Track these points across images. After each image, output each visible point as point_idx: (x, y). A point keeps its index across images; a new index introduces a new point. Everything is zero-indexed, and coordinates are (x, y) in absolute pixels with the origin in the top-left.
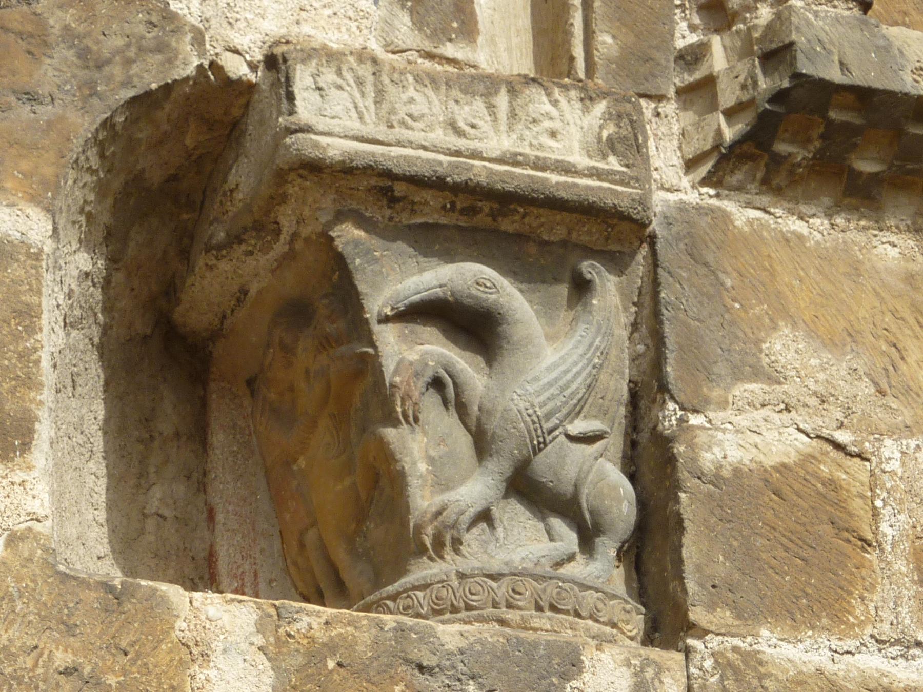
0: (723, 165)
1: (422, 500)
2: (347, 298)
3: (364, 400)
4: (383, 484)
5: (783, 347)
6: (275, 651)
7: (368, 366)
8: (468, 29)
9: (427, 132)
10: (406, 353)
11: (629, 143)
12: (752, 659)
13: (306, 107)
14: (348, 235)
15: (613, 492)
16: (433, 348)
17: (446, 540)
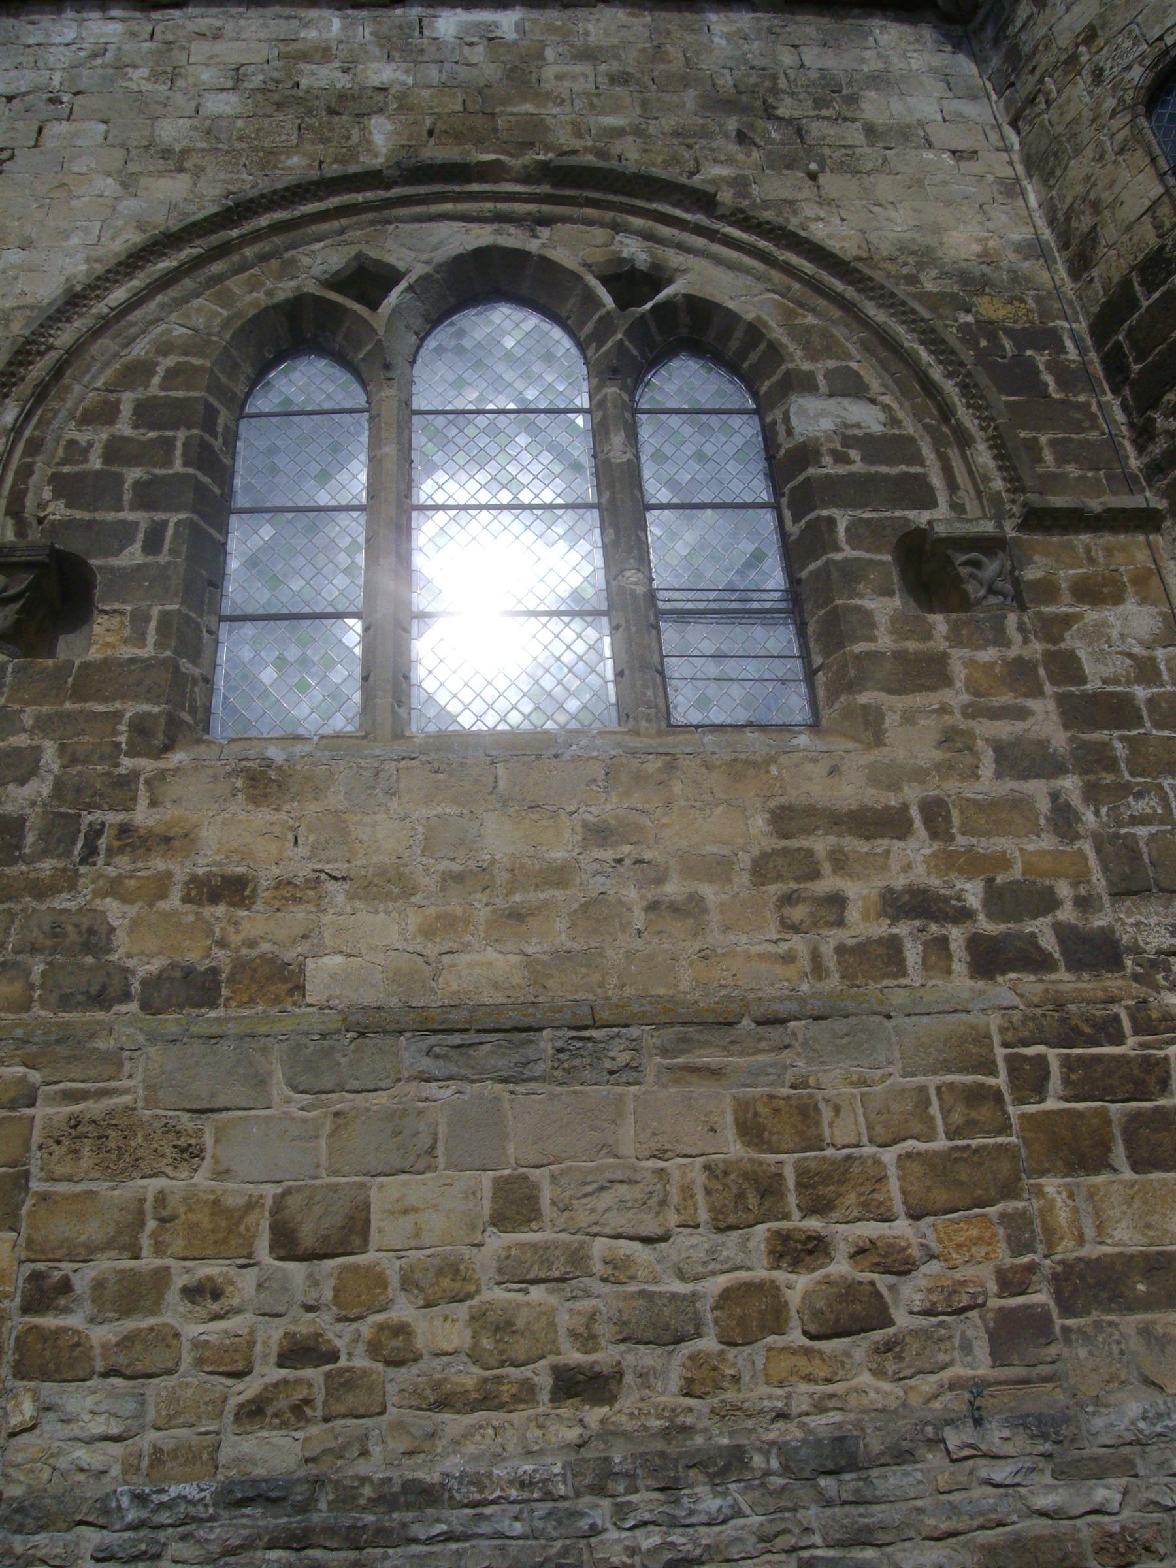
0: (1020, 528)
1: (972, 596)
2: (951, 563)
3: (958, 580)
4: (965, 595)
5: (1036, 558)
6: (948, 622)
7: (958, 574)
8: (965, 512)
9: (961, 529)
10: (964, 571)
11: (1000, 526)
12: (1041, 613)
13: (937, 529)
14: (949, 552)
15: (1009, 587)
16: (969, 569)
17: (979, 602)
